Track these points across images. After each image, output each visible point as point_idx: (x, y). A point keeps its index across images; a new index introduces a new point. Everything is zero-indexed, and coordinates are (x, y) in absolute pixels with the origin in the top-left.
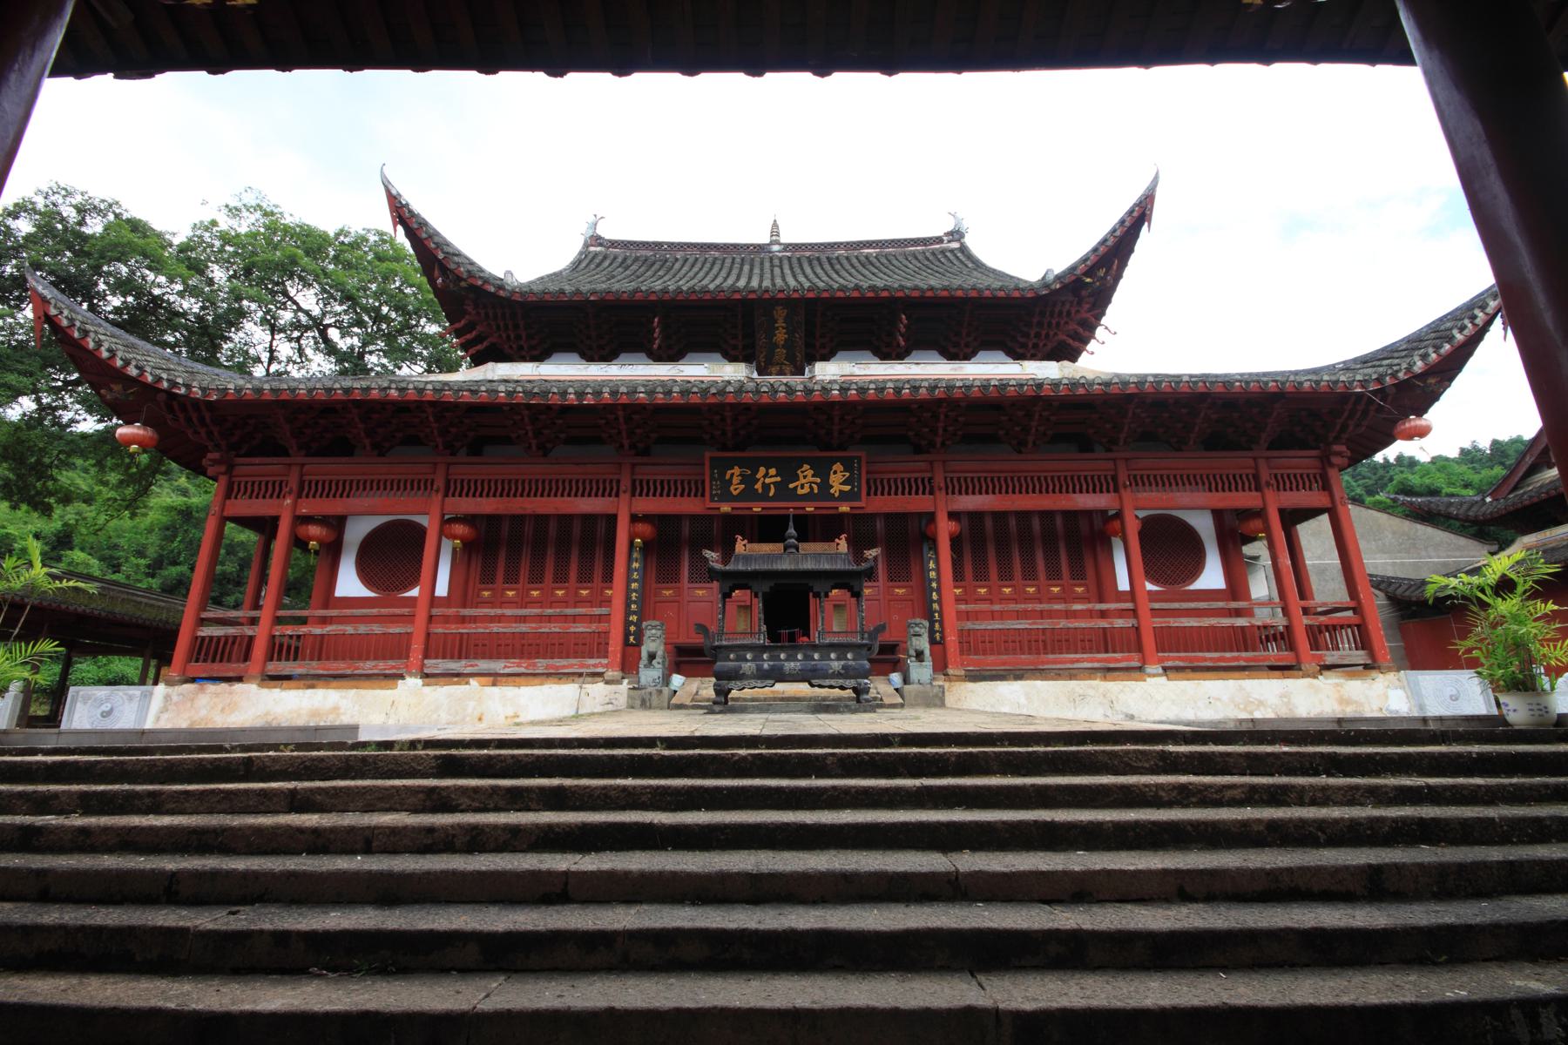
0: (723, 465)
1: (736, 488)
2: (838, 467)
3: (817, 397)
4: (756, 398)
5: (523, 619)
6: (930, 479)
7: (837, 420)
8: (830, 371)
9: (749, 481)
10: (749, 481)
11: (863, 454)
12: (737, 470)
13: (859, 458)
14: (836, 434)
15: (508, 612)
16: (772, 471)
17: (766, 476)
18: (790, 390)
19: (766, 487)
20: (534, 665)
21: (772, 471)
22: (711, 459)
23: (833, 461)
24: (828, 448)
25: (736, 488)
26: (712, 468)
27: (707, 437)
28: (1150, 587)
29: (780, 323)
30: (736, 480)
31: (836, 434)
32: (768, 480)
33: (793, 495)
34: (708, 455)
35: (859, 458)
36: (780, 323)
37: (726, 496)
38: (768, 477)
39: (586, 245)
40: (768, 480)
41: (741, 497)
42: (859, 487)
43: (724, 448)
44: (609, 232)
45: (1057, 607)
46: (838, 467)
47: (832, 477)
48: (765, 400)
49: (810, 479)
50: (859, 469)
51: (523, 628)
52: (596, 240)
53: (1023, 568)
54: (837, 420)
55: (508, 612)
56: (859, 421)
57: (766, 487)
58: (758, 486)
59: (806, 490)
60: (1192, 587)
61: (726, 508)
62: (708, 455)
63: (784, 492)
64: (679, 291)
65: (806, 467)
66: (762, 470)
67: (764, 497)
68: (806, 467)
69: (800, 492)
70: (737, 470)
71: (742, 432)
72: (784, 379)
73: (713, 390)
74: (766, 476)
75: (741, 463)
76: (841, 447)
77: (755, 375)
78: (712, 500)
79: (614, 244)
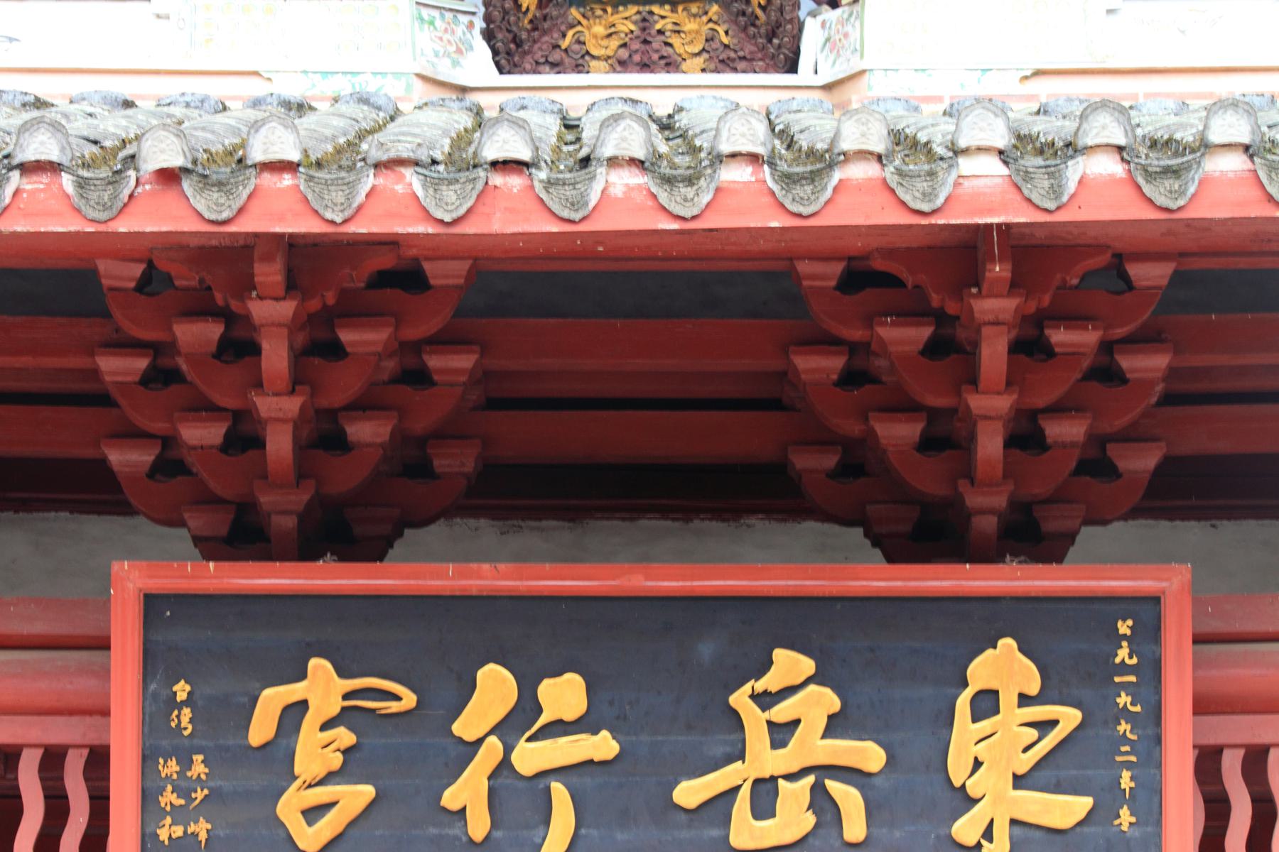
0: (213, 650)
2: (1003, 666)
3: (857, 202)
4: (449, 204)
7: (994, 353)
11: (1169, 582)
12: (323, 686)
13: (1147, 610)
14: (990, 446)
17: (522, 719)
18: (680, 155)
21: (564, 695)
22: (153, 604)
23: (984, 621)
24: (931, 533)
26: (156, 663)
27: (127, 459)
30: (316, 751)
31: (990, 446)
32: (531, 756)
34: (131, 579)
35: (1147, 610)
40: (531, 756)
42: (1149, 801)
43: (244, 537)
46: (1003, 666)
47: (965, 730)
48: (514, 214)
49: (813, 746)
50: (1151, 671)
54: (994, 353)
56: (1147, 365)
57: (519, 798)
58: (467, 792)
62: (131, 579)
65: (789, 665)
66: (495, 687)
68: (789, 665)
70: (323, 686)
71: (367, 432)
72: (659, 92)
73: (163, 152)
74: (522, 719)
75: (350, 633)
76: (1030, 537)
77: (478, 65)
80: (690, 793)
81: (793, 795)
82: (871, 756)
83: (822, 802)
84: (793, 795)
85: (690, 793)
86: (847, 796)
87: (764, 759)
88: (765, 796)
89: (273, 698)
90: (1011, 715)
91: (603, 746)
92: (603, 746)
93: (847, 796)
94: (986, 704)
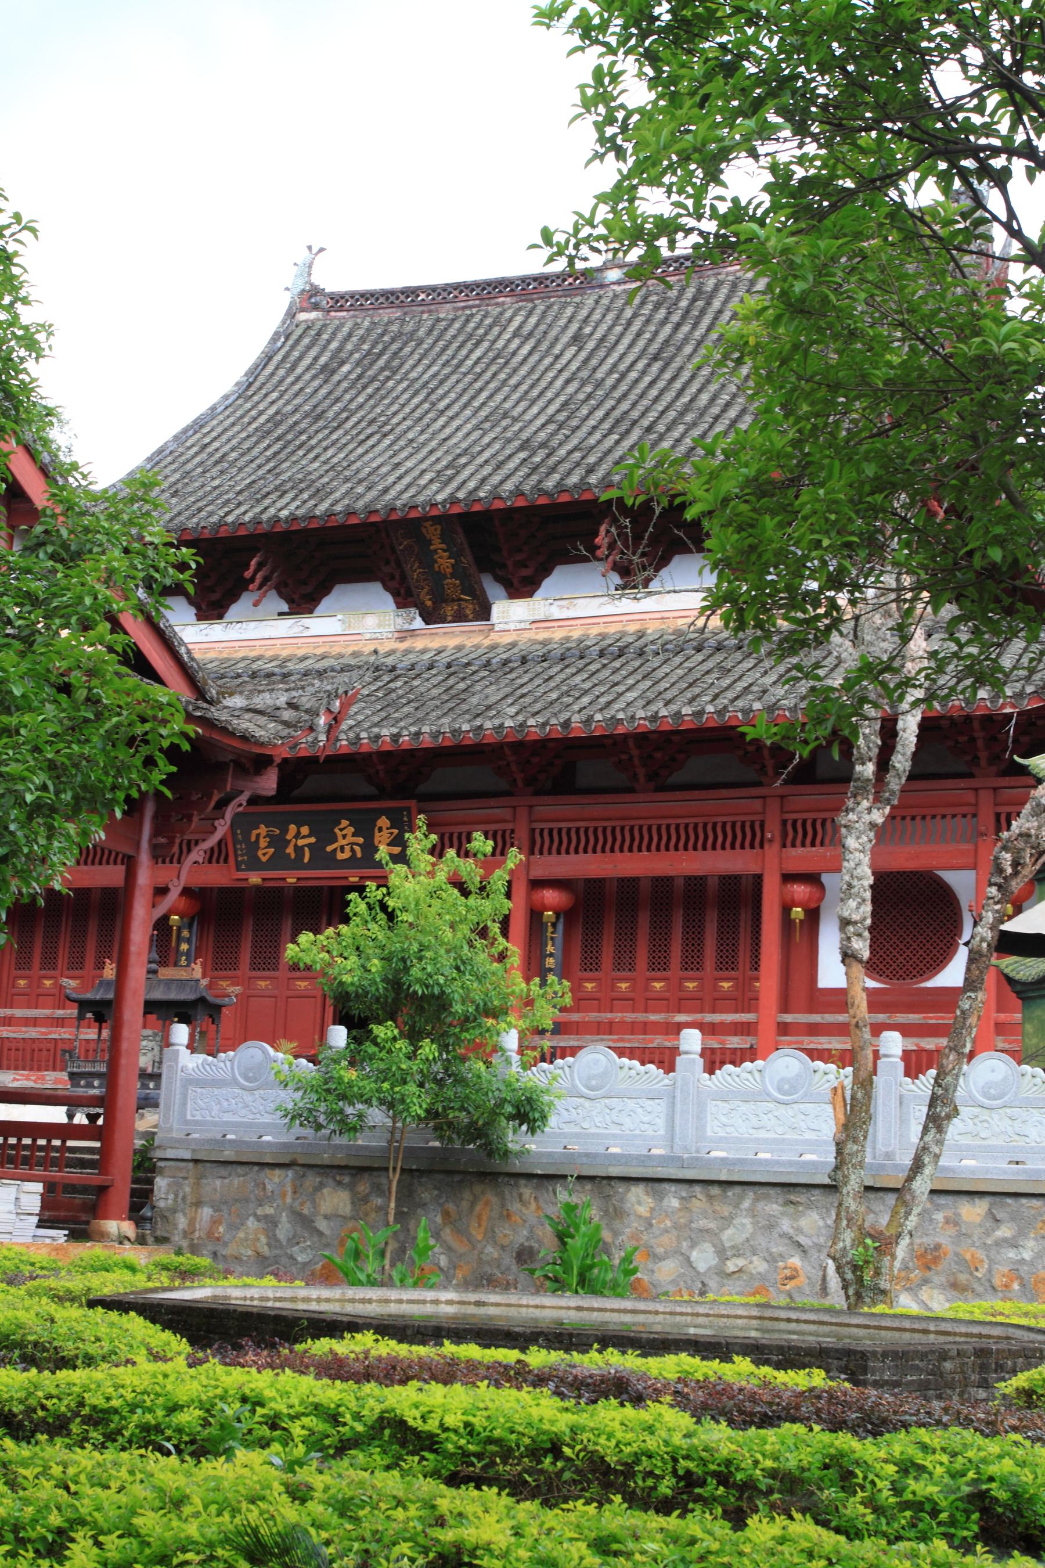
1: (265, 853)
2: (383, 822)
5: (34, 1022)
6: (513, 831)
8: (513, 617)
9: (278, 842)
10: (278, 842)
12: (263, 830)
15: (18, 1013)
16: (305, 830)
17: (298, 836)
19: (299, 850)
20: (43, 1078)
21: (305, 830)
25: (265, 853)
28: (871, 984)
29: (437, 544)
30: (263, 843)
32: (301, 842)
33: (330, 861)
36: (437, 544)
37: (254, 864)
38: (301, 838)
39: (291, 314)
40: (301, 842)
41: (273, 864)
44: (334, 279)
45: (653, 1017)
46: (383, 822)
47: (377, 834)
49: (350, 839)
51: (33, 1033)
52: (311, 297)
53: (685, 951)
55: (18, 1013)
57: (299, 850)
58: (290, 850)
59: (347, 855)
60: (930, 984)
61: (255, 879)
63: (322, 857)
64: (276, 520)
65: (344, 823)
66: (293, 828)
67: (297, 863)
68: (344, 823)
69: (340, 856)
70: (263, 830)
74: (298, 836)
78: (238, 869)
79: (338, 301)
80: (329, 849)
81: (347, 848)
82: (361, 840)
83: (352, 850)
84: (347, 848)
85: (329, 849)
86: (357, 849)
87: (344, 842)
88: (342, 849)
89: (255, 832)
90: (385, 831)
91: (313, 840)
92: (313, 840)
93: (357, 849)
94: (380, 830)
